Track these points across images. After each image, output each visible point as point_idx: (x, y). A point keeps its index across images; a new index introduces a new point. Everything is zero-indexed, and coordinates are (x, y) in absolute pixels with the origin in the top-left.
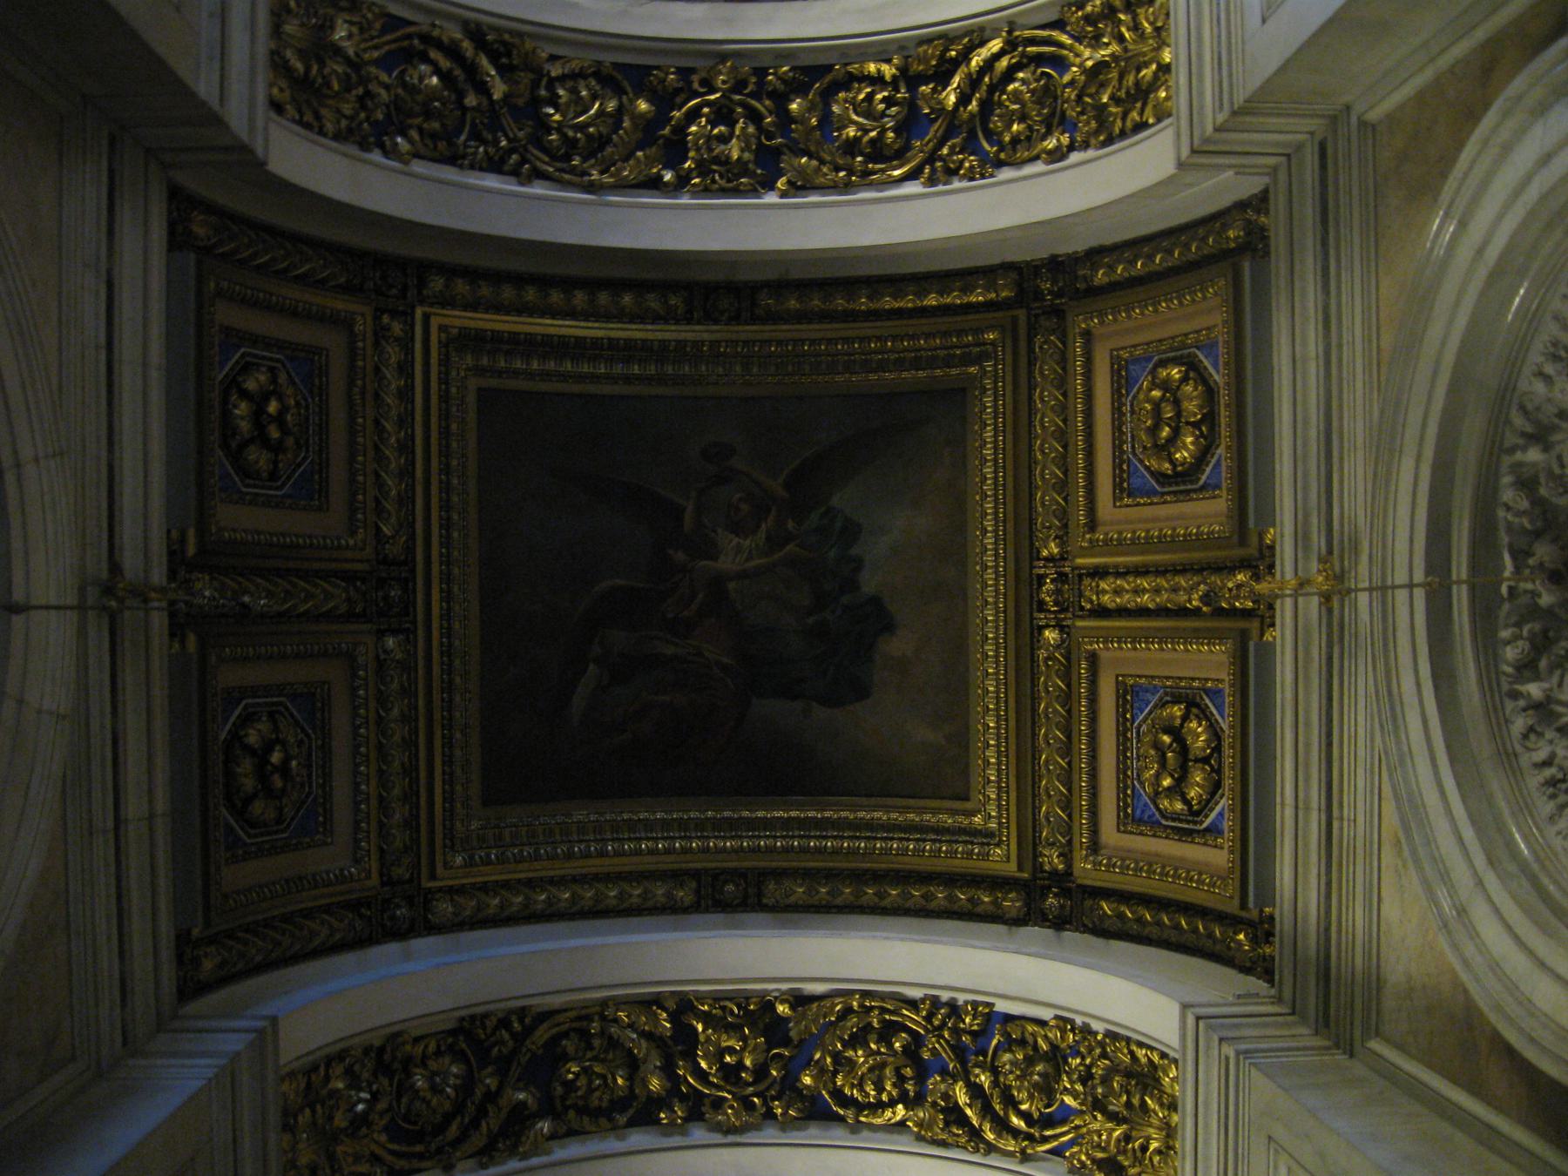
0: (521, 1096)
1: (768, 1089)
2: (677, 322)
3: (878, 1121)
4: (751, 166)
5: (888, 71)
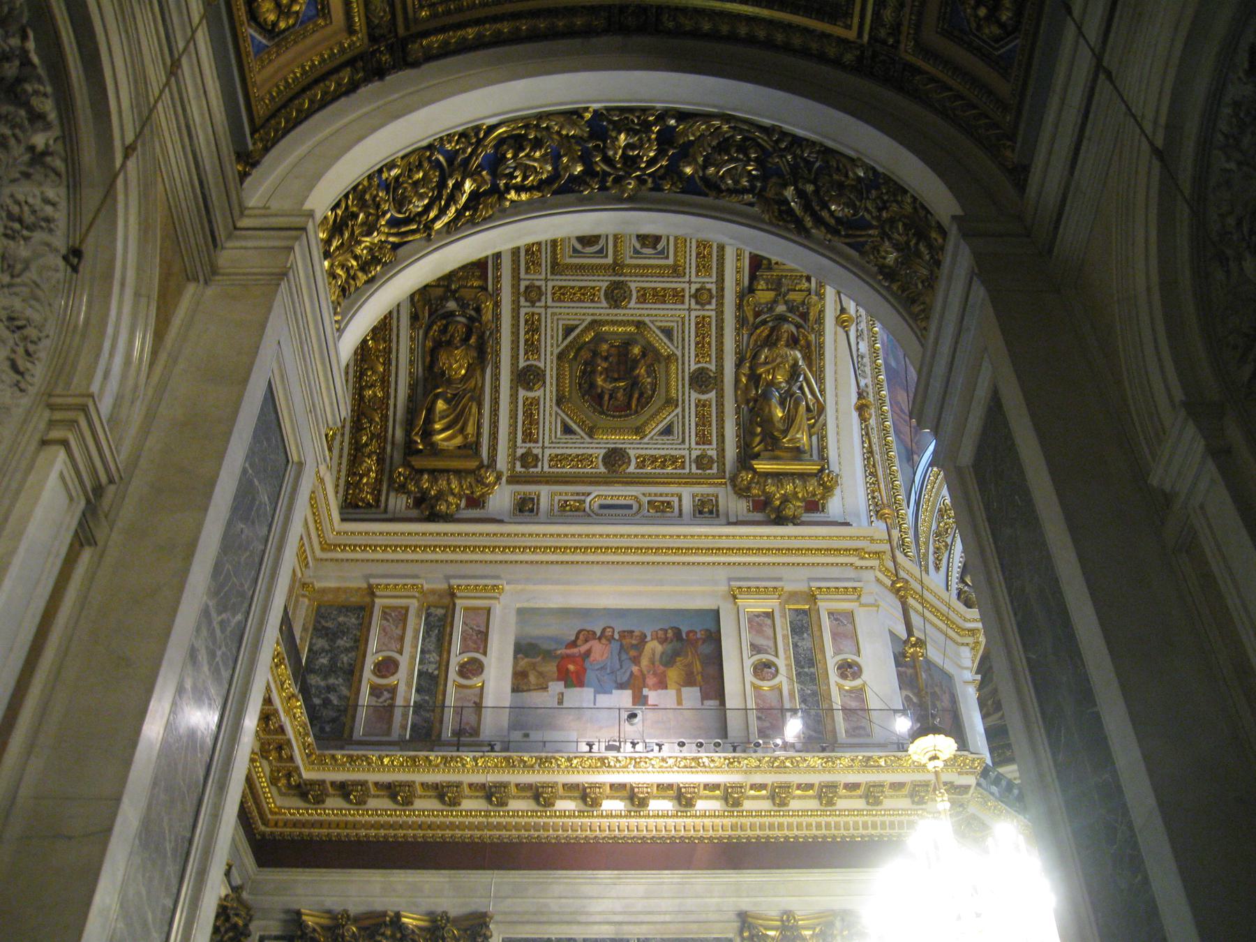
4: (611, 127)
5: (512, 195)
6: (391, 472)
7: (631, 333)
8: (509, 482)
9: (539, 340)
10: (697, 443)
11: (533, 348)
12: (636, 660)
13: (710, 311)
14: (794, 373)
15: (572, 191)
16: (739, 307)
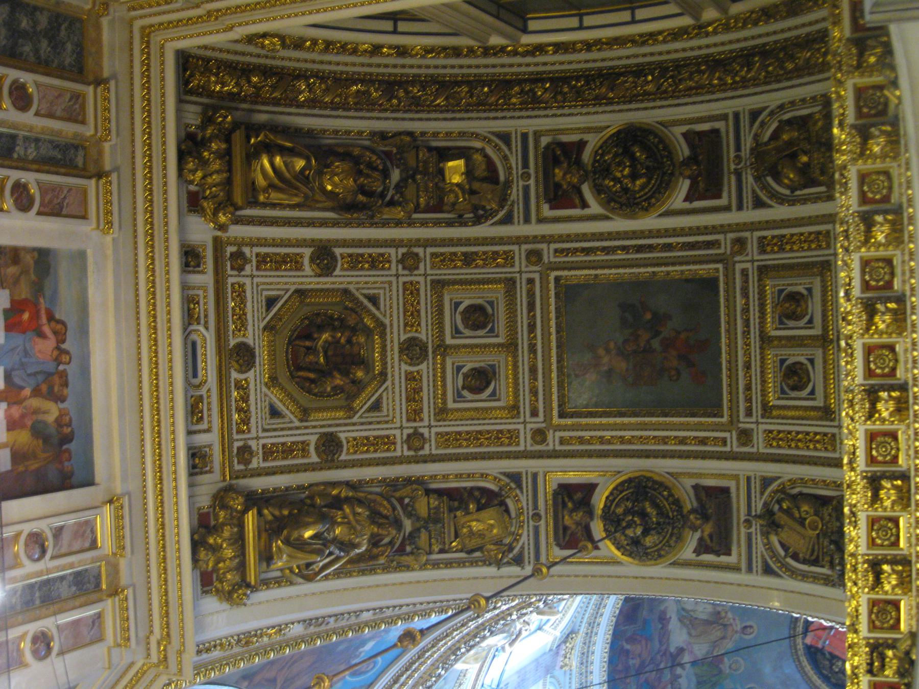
6: (228, 109)
7: (374, 371)
8: (216, 240)
9: (362, 269)
10: (264, 446)
11: (355, 262)
12: (36, 392)
13: (401, 450)
14: (346, 546)
16: (408, 481)
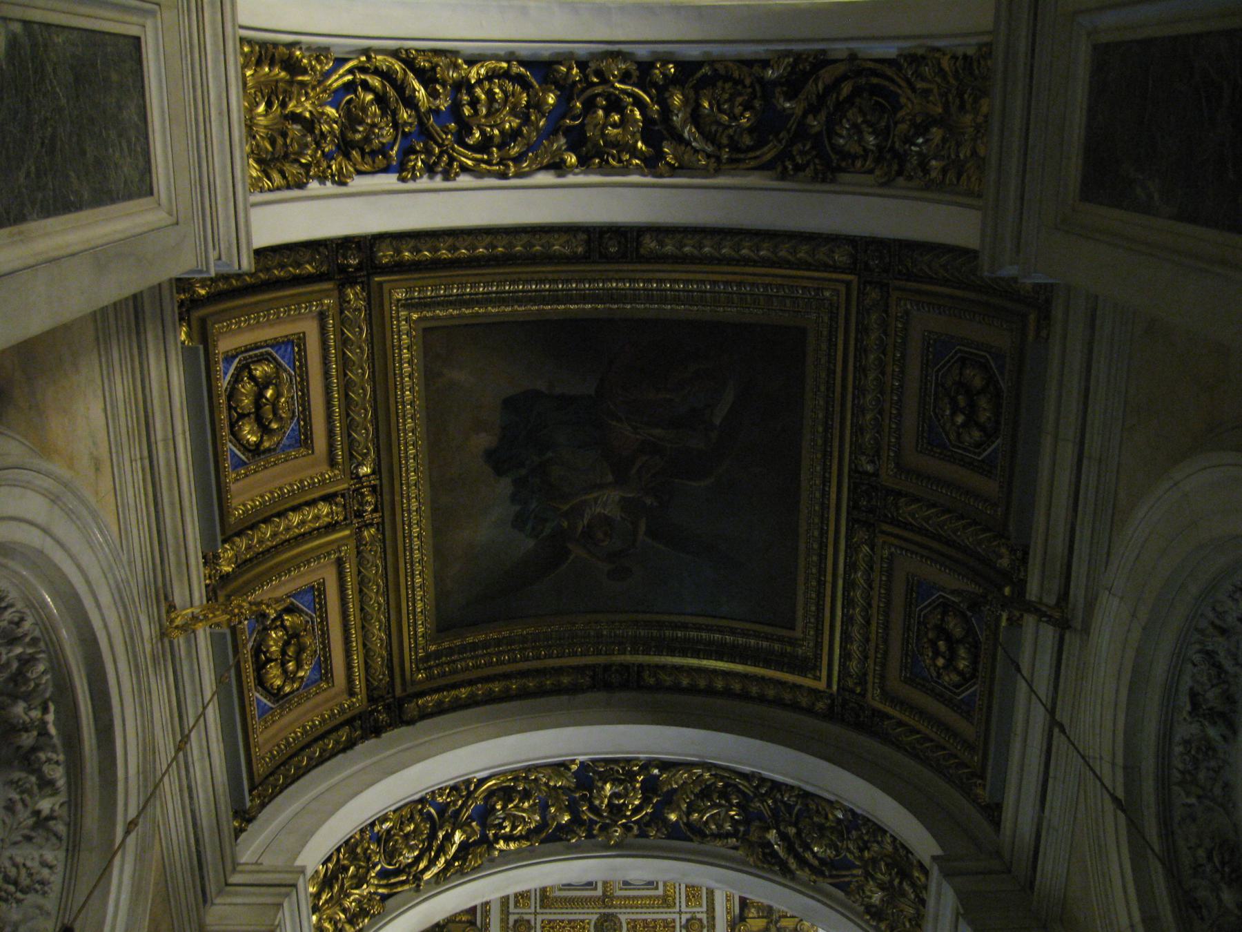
0: (788, 105)
1: (583, 90)
2: (649, 665)
3: (492, 64)
5: (501, 845)
15: (561, 839)
